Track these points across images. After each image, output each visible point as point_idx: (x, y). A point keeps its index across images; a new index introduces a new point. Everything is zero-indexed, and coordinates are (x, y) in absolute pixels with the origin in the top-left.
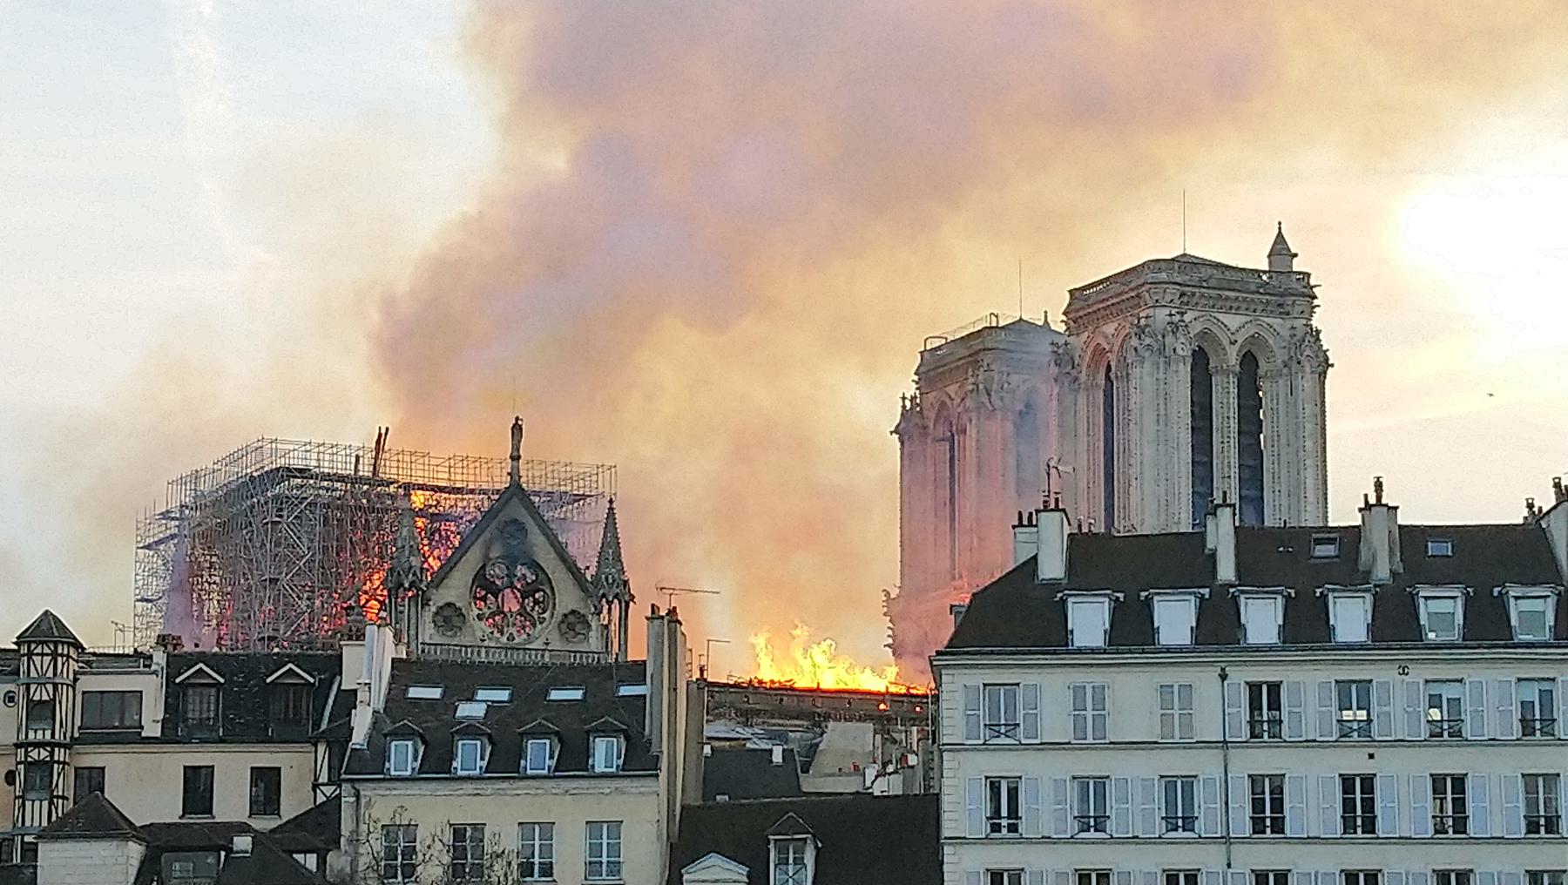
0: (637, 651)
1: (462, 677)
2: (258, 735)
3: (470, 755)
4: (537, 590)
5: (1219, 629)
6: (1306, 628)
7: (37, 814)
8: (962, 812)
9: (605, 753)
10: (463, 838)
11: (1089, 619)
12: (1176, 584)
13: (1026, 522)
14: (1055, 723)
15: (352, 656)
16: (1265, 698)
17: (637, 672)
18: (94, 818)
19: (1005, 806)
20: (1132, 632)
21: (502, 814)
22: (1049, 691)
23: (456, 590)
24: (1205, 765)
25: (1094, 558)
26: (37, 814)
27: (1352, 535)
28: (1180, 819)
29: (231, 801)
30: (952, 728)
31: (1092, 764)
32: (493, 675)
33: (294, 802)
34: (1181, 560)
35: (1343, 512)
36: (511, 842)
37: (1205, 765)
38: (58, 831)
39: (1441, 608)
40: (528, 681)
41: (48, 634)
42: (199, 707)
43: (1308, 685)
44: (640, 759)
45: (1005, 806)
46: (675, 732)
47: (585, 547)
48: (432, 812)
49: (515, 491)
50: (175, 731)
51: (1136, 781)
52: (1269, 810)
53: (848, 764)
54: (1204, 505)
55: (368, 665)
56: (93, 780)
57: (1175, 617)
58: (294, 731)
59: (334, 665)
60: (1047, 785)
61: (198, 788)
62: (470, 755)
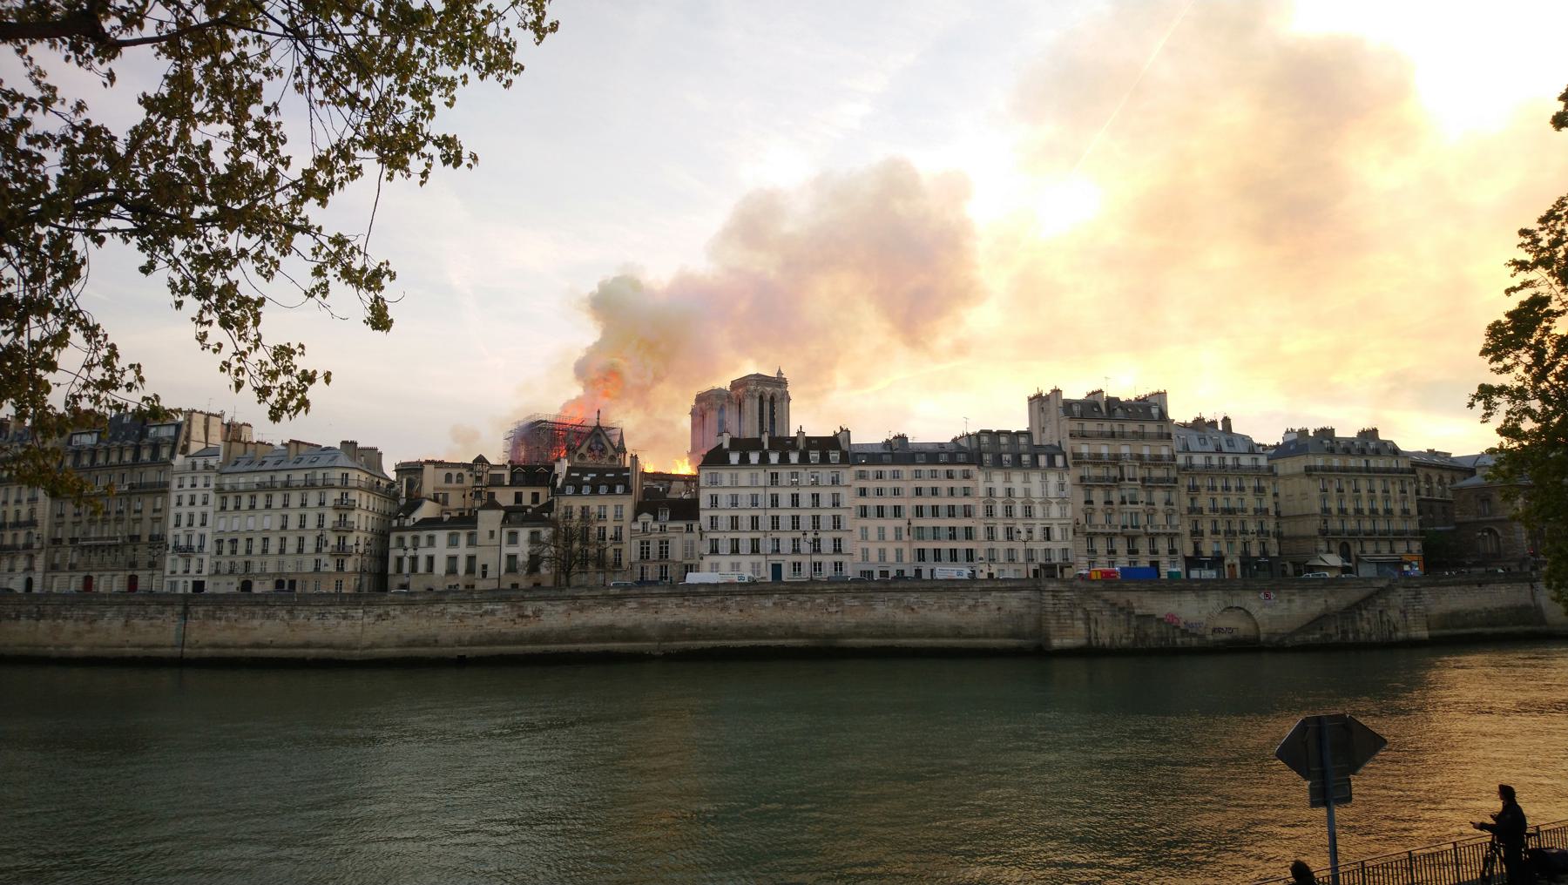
0: (628, 464)
1: (584, 471)
2: (533, 485)
3: (586, 490)
4: (603, 450)
5: (764, 460)
6: (784, 460)
7: (478, 504)
8: (704, 502)
9: (619, 489)
10: (585, 510)
11: (734, 458)
12: (754, 450)
13: (720, 435)
14: (726, 482)
15: (557, 466)
16: (774, 476)
17: (627, 470)
18: (492, 504)
19: (714, 501)
20: (744, 461)
21: (594, 504)
22: (725, 475)
23: (583, 450)
24: (761, 492)
25: (736, 444)
26: (478, 504)
27: (795, 439)
28: (755, 504)
29: (527, 500)
30: (702, 484)
31: (734, 491)
32: (592, 470)
33: (542, 501)
34: (755, 444)
35: (793, 434)
36: (596, 510)
37: (761, 492)
38: (483, 508)
39: (814, 455)
40: (601, 472)
41: (480, 460)
42: (519, 478)
43: (784, 473)
44: (628, 490)
45: (714, 501)
46: (636, 484)
47: (616, 440)
48: (577, 503)
49: (598, 426)
50: (512, 484)
51: (745, 494)
52: (775, 501)
53: (679, 492)
54: (762, 431)
55: (562, 467)
56: (492, 495)
57: (754, 457)
58: (541, 485)
59: (553, 468)
60: (724, 496)
61: (518, 497)
62: (586, 490)
